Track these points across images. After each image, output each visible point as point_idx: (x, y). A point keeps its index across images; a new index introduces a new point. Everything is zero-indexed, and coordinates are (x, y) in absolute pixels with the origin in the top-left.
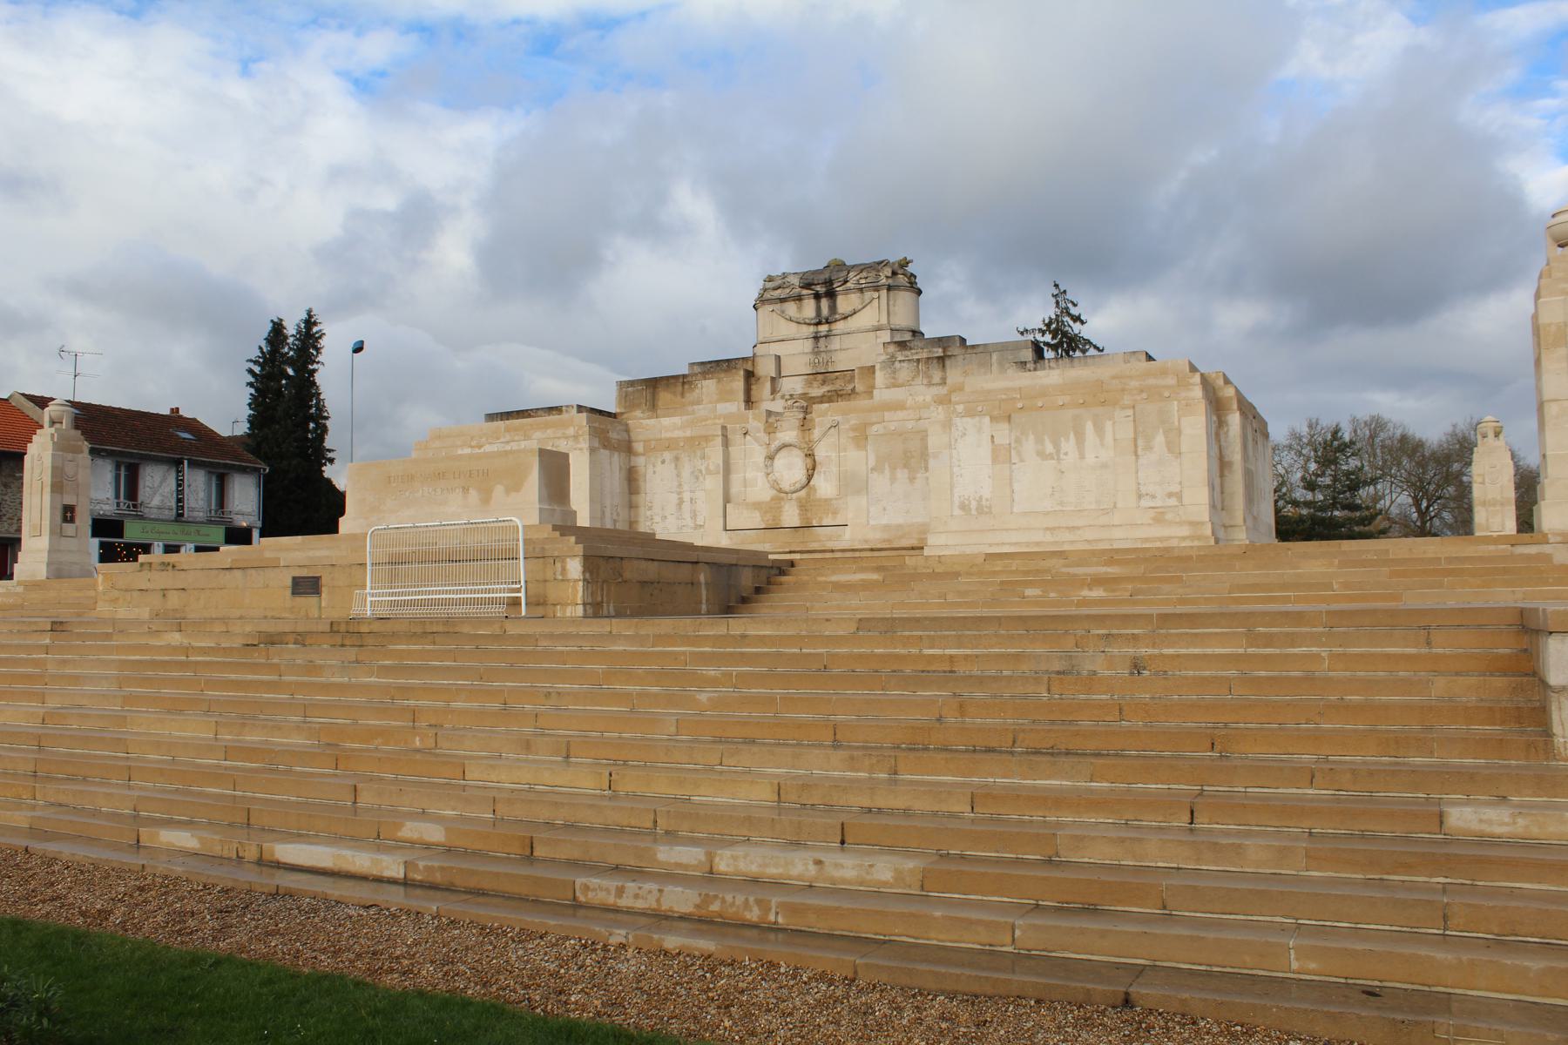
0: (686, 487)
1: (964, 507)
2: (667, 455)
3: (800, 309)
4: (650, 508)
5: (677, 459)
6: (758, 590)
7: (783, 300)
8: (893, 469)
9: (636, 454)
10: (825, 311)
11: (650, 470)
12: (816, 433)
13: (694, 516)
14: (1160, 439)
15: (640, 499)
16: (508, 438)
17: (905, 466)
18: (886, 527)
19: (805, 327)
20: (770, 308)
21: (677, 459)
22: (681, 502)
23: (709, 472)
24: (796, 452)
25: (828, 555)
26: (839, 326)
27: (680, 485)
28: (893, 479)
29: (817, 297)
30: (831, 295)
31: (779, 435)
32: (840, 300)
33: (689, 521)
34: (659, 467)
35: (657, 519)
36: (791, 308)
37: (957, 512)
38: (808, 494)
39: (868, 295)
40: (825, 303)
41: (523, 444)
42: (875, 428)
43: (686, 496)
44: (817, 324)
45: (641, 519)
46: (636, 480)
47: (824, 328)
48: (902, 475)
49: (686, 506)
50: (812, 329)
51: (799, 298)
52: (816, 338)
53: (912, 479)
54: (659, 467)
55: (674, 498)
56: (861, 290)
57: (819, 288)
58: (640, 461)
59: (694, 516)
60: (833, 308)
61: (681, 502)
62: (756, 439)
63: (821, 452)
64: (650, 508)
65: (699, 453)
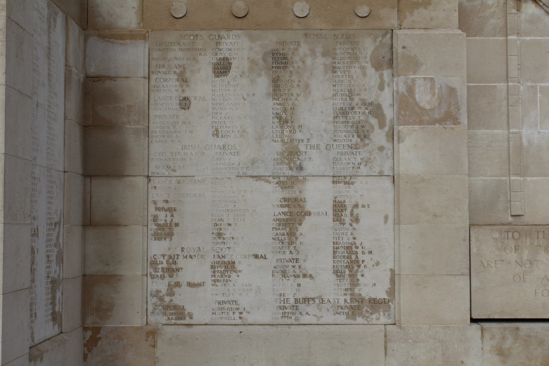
0: (314, 162)
2: (238, 46)
4: (166, 231)
5: (278, 61)
6: (154, 342)
9: (112, 35)
11: (168, 91)
13: (349, 263)
15: (144, 194)
21: (278, 61)
22: (293, 216)
23: (409, 110)
27: (291, 154)
33: (326, 283)
34: (203, 85)
35: (194, 270)
43: (318, 194)
45: (133, 270)
46: (110, 126)
49: (317, 235)
54: (203, 85)
55: (267, 200)
58: (130, 59)
59: (349, 263)
61: (293, 216)
64: (166, 231)
65: (368, 46)
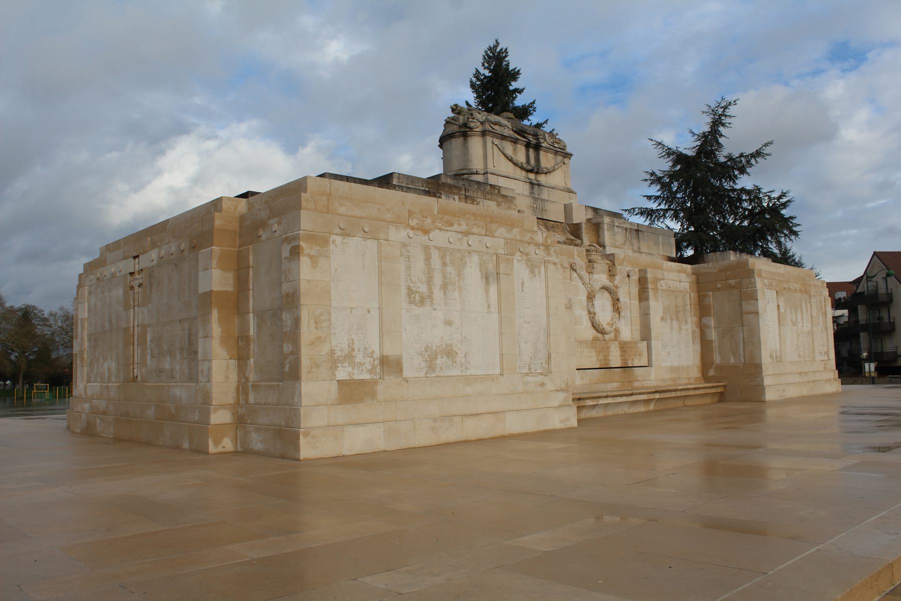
1: (771, 356)
3: (515, 150)
7: (503, 137)
8: (672, 319)
10: (532, 161)
12: (618, 279)
14: (821, 319)
16: (464, 227)
17: (677, 318)
18: (673, 369)
19: (518, 170)
20: (497, 142)
24: (607, 295)
25: (673, 394)
26: (542, 179)
28: (672, 328)
29: (528, 145)
30: (537, 147)
31: (596, 276)
32: (542, 153)
36: (508, 148)
37: (770, 360)
38: (616, 336)
39: (560, 158)
40: (532, 152)
41: (488, 241)
42: (662, 282)
44: (531, 171)
47: (532, 176)
48: (675, 324)
50: (524, 173)
51: (515, 141)
52: (532, 184)
53: (680, 329)
56: (556, 153)
57: (534, 141)
60: (537, 160)
62: (581, 278)
63: (622, 295)
